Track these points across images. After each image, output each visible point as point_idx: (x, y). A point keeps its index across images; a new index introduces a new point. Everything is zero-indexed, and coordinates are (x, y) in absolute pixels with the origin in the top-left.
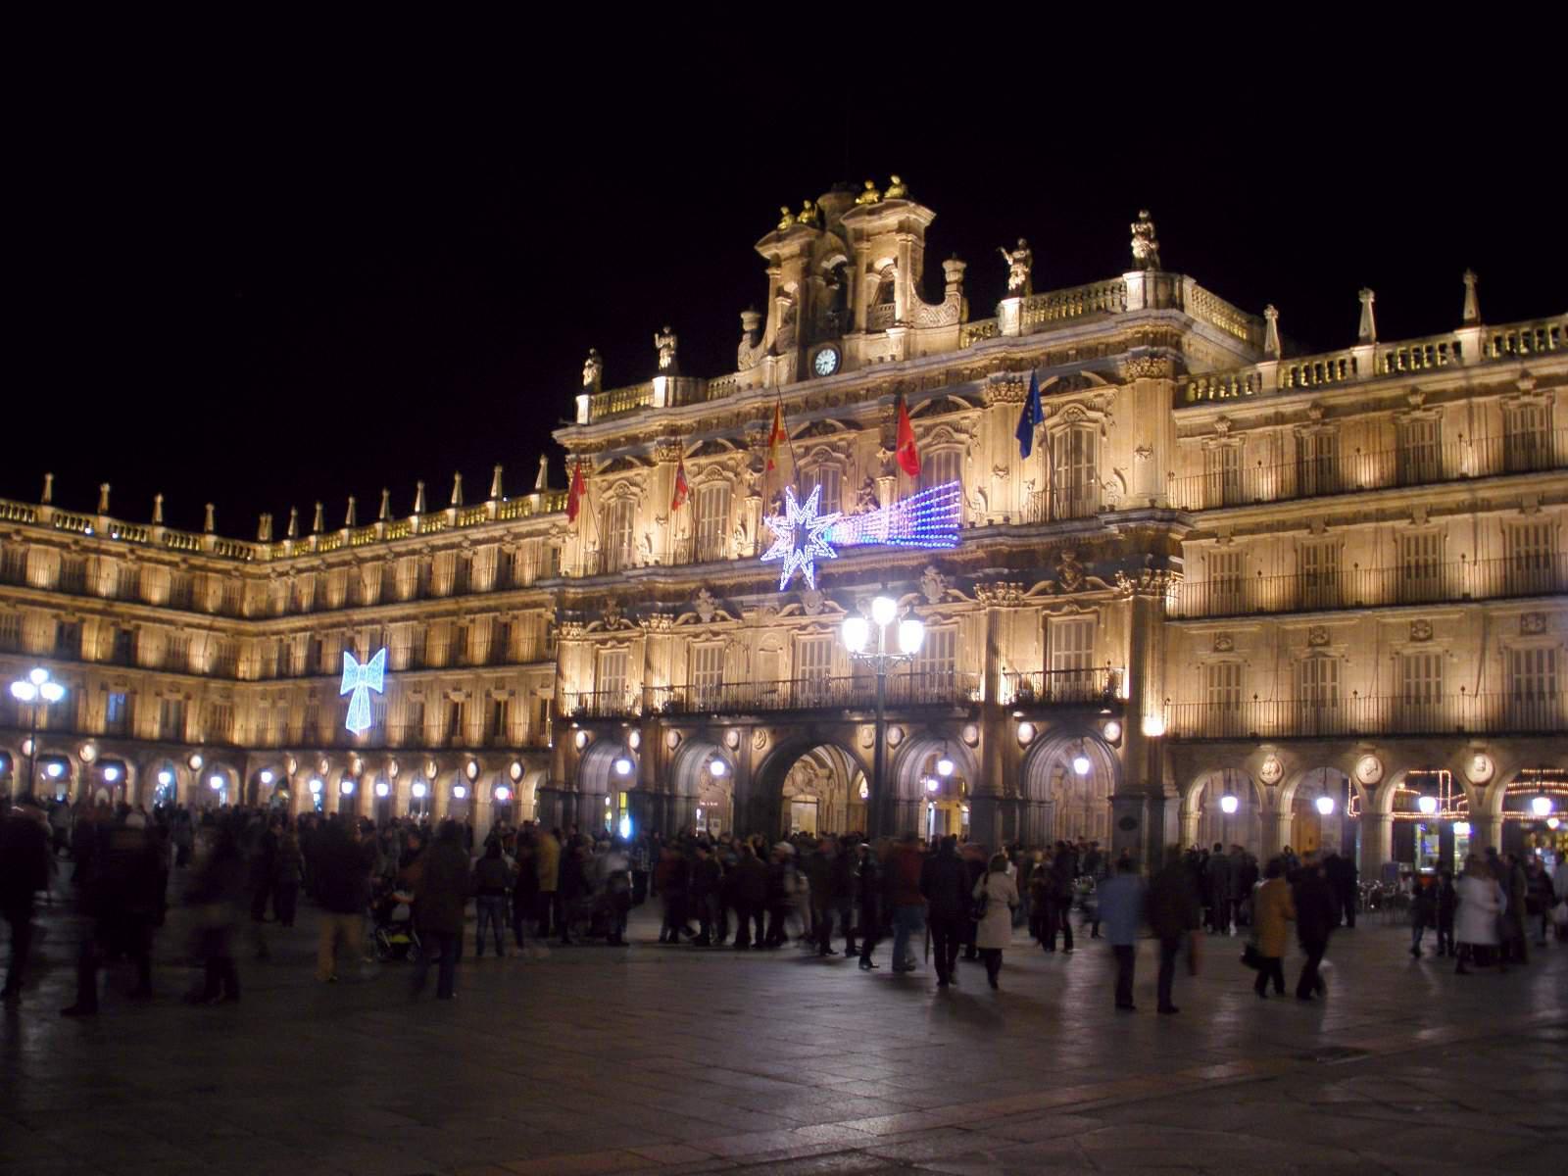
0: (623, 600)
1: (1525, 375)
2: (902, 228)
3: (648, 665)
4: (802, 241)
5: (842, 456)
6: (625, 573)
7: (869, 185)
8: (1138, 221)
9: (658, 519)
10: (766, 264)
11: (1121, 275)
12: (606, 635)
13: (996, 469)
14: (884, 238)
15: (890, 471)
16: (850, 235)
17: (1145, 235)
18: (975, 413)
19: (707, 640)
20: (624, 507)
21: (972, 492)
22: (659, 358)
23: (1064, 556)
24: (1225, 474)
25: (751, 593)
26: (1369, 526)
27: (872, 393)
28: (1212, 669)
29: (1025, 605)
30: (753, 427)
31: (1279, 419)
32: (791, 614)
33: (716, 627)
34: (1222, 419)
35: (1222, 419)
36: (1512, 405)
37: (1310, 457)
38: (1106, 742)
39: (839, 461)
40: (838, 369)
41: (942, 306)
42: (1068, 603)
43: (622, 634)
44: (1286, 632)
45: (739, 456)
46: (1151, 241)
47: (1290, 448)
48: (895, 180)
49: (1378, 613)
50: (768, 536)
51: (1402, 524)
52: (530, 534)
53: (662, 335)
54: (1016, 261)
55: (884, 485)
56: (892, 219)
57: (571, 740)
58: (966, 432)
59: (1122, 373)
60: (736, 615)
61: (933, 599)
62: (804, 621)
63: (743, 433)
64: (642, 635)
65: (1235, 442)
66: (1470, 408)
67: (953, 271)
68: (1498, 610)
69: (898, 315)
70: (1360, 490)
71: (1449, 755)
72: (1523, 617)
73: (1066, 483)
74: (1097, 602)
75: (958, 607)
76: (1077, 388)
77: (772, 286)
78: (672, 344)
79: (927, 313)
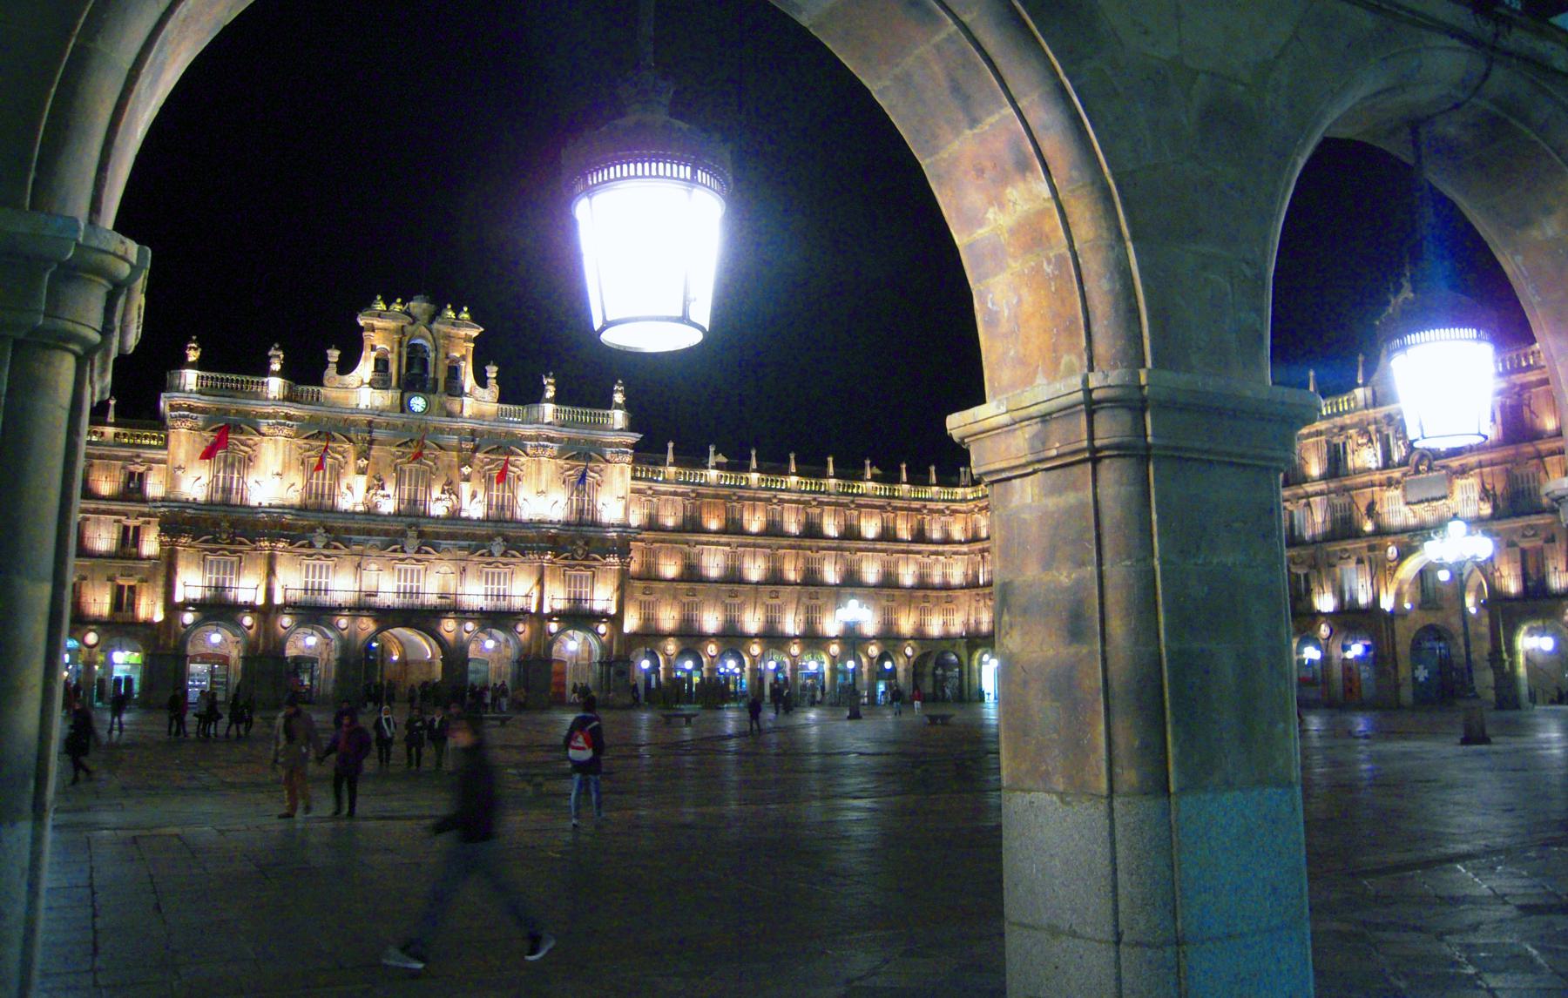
0: (233, 524)
1: (775, 497)
2: (467, 339)
3: (271, 573)
4: (400, 324)
5: (431, 463)
6: (260, 510)
7: (449, 306)
8: (620, 385)
9: (278, 474)
10: (362, 329)
11: (610, 409)
12: (218, 546)
13: (542, 492)
14: (457, 341)
15: (467, 479)
16: (434, 331)
17: (621, 391)
18: (523, 459)
19: (319, 559)
20: (234, 457)
21: (520, 500)
22: (270, 364)
23: (578, 542)
24: (650, 514)
25: (359, 534)
26: (714, 547)
27: (452, 431)
28: (641, 602)
29: (552, 563)
30: (364, 431)
31: (675, 494)
32: (395, 551)
33: (326, 552)
34: (650, 488)
35: (650, 488)
36: (769, 507)
37: (689, 514)
38: (598, 634)
39: (428, 465)
40: (427, 411)
41: (487, 391)
42: (578, 565)
43: (232, 547)
44: (676, 589)
45: (346, 446)
46: (624, 396)
47: (680, 509)
48: (466, 309)
49: (718, 585)
50: (371, 501)
51: (727, 548)
52: (100, 457)
53: (276, 349)
54: (549, 383)
55: (466, 489)
56: (463, 332)
57: (178, 617)
58: (517, 467)
59: (608, 457)
60: (346, 547)
61: (496, 554)
62: (401, 556)
63: (349, 431)
64: (256, 550)
65: (655, 500)
66: (754, 505)
67: (492, 371)
68: (761, 588)
69: (467, 390)
70: (708, 532)
71: (743, 644)
72: (771, 592)
73: (577, 505)
74: (594, 567)
75: (513, 560)
76: (585, 460)
77: (367, 344)
78: (282, 356)
79: (479, 391)
